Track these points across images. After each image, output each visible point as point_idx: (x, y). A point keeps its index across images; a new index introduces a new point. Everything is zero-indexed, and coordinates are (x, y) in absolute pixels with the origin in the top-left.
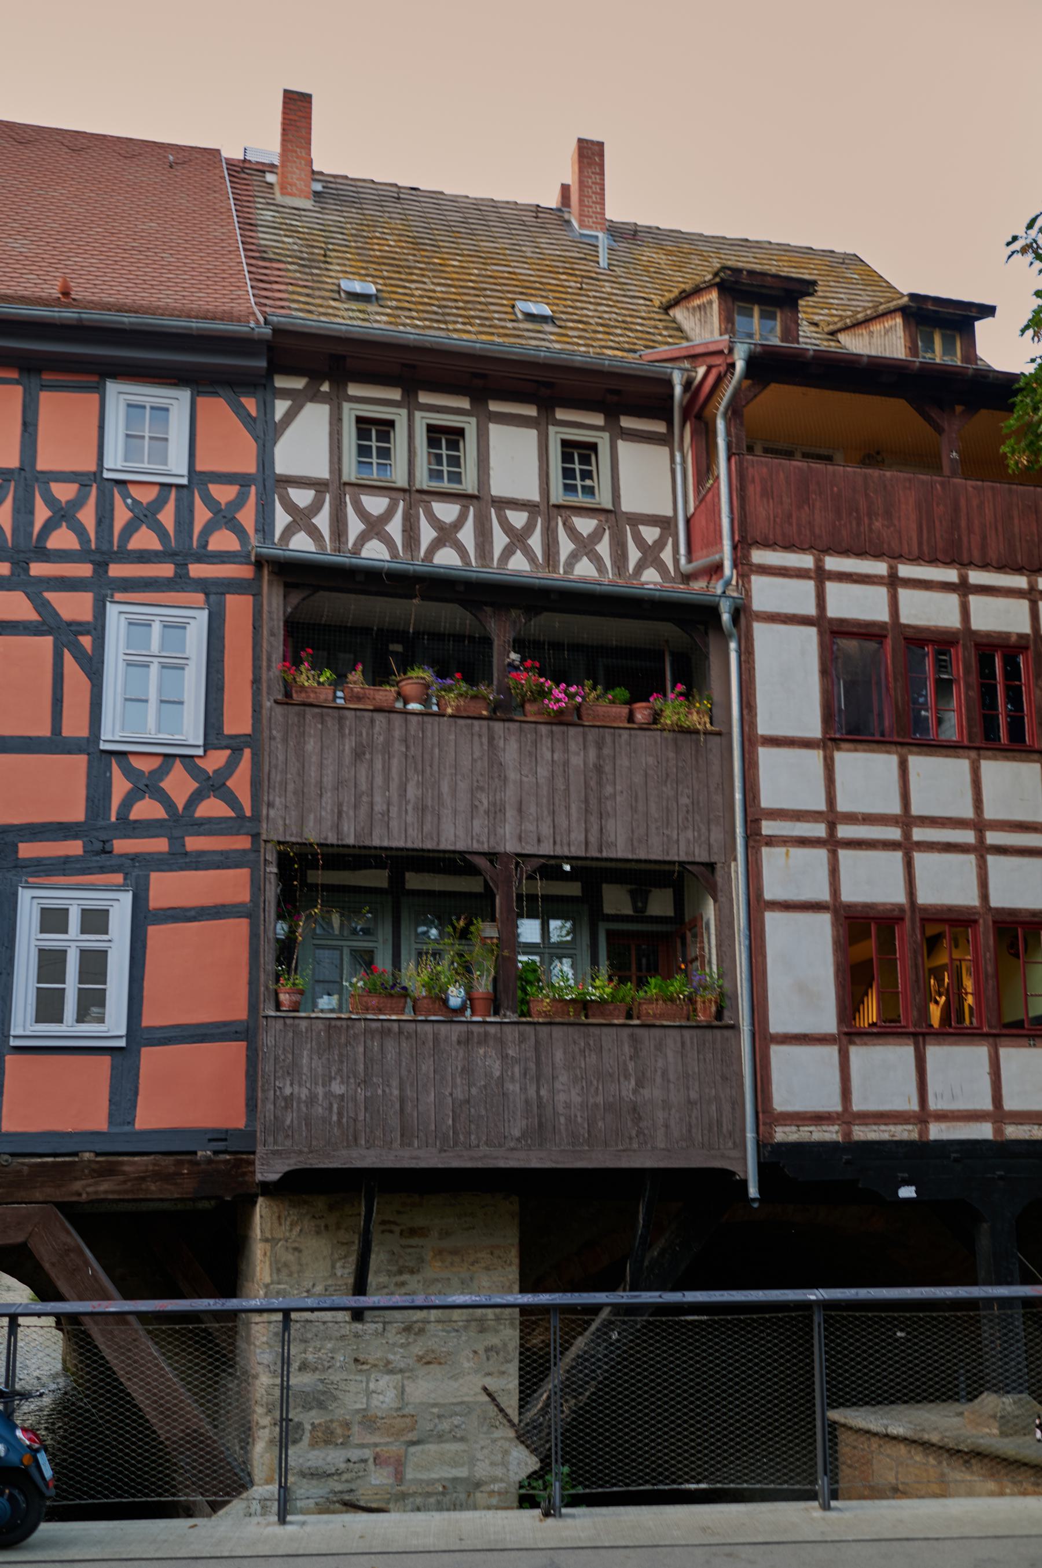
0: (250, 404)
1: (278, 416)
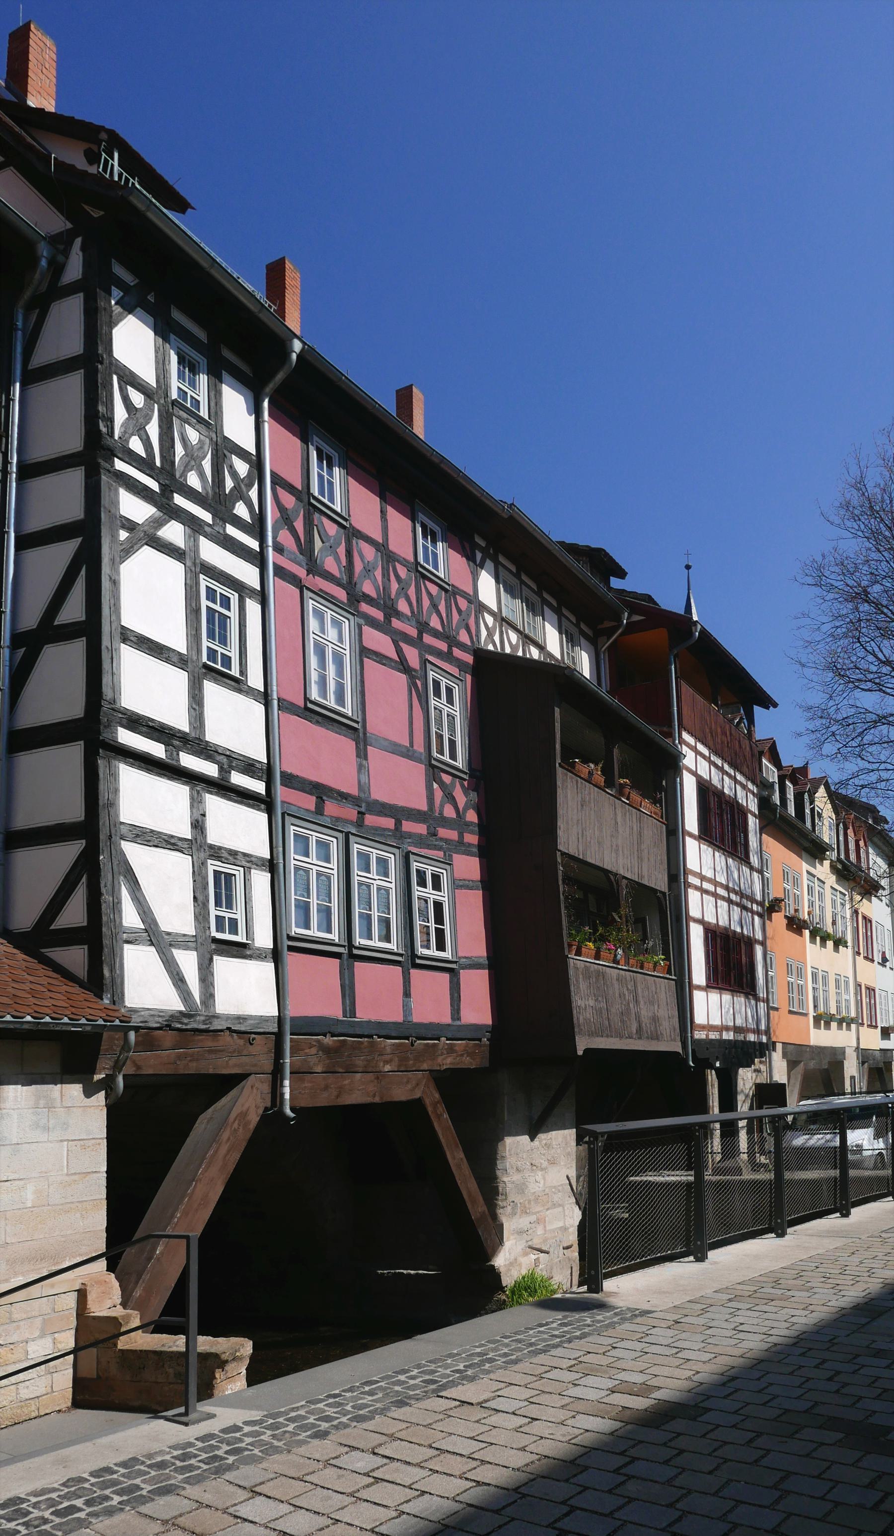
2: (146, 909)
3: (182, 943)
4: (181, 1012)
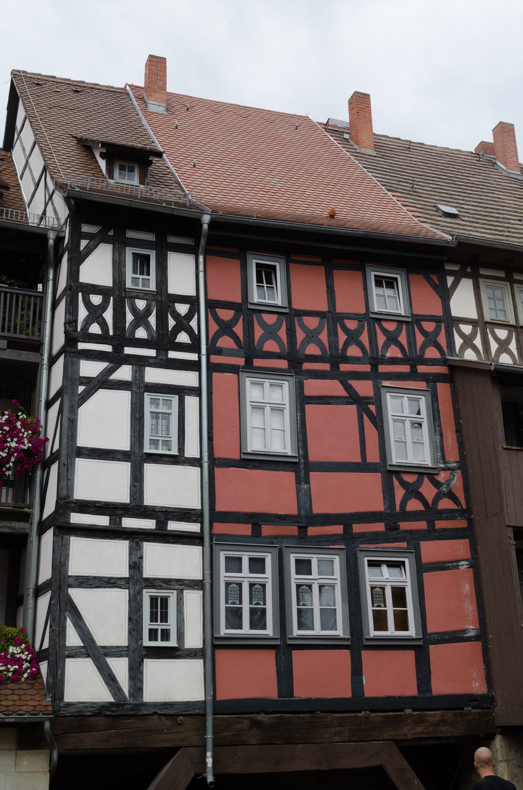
0: (435, 278)
1: (449, 284)
2: (86, 632)
3: (115, 653)
4: (111, 703)
